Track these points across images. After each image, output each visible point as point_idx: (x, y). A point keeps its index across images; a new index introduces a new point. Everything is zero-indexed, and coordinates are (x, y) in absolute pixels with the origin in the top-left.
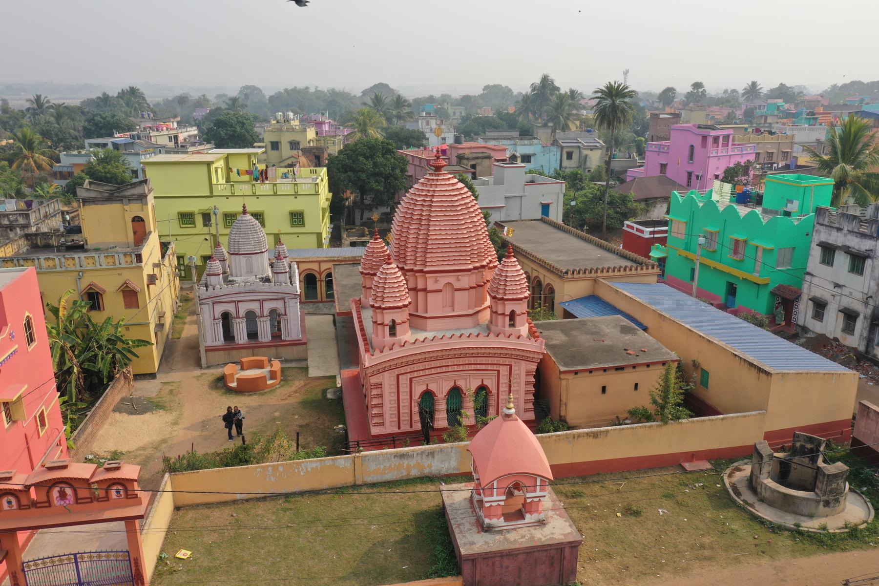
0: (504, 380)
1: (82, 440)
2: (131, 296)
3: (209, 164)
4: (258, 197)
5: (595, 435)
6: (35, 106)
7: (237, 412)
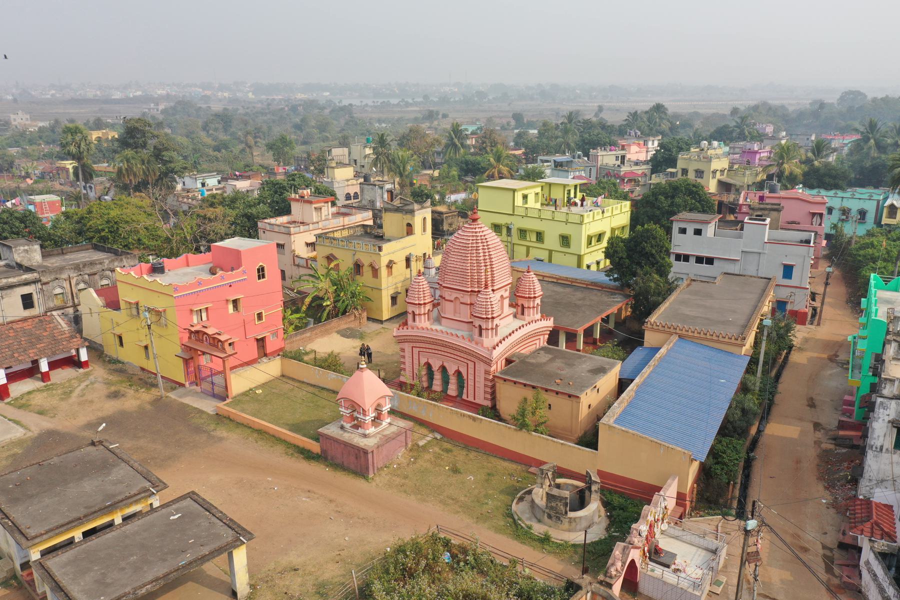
0: (471, 371)
1: (298, 338)
2: (375, 272)
3: (514, 191)
4: (542, 219)
5: (474, 419)
6: (566, 121)
7: (369, 348)
